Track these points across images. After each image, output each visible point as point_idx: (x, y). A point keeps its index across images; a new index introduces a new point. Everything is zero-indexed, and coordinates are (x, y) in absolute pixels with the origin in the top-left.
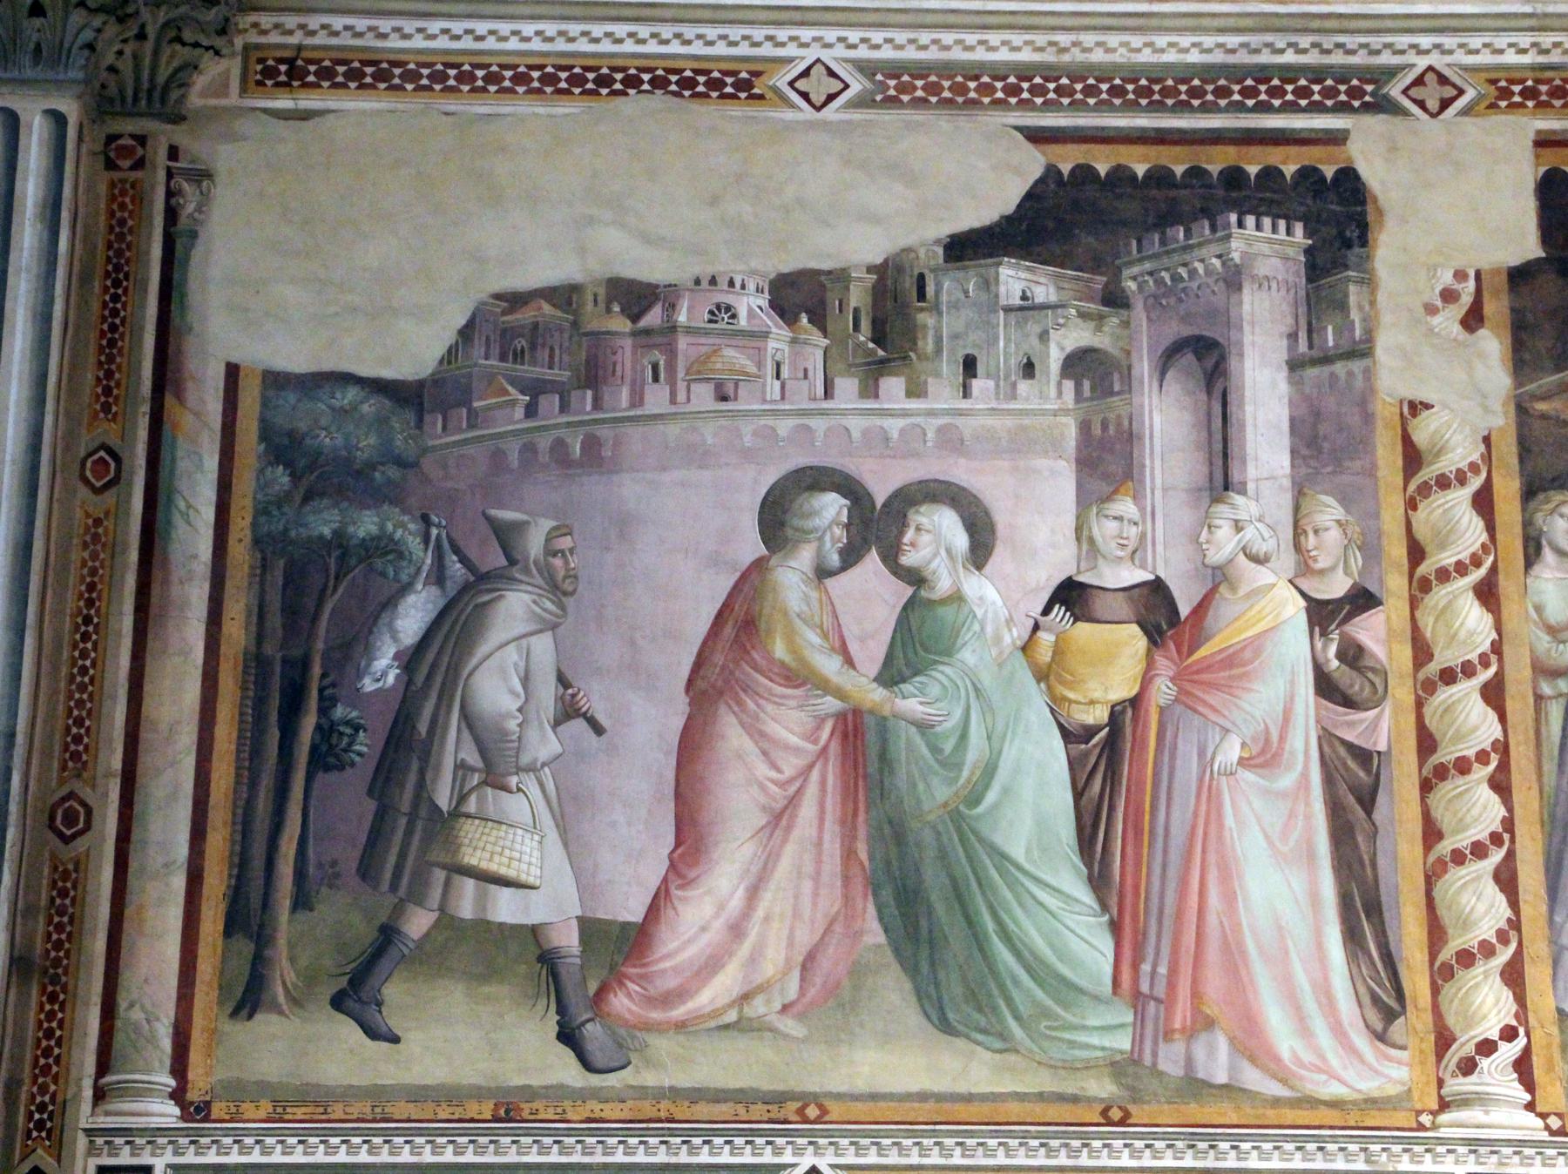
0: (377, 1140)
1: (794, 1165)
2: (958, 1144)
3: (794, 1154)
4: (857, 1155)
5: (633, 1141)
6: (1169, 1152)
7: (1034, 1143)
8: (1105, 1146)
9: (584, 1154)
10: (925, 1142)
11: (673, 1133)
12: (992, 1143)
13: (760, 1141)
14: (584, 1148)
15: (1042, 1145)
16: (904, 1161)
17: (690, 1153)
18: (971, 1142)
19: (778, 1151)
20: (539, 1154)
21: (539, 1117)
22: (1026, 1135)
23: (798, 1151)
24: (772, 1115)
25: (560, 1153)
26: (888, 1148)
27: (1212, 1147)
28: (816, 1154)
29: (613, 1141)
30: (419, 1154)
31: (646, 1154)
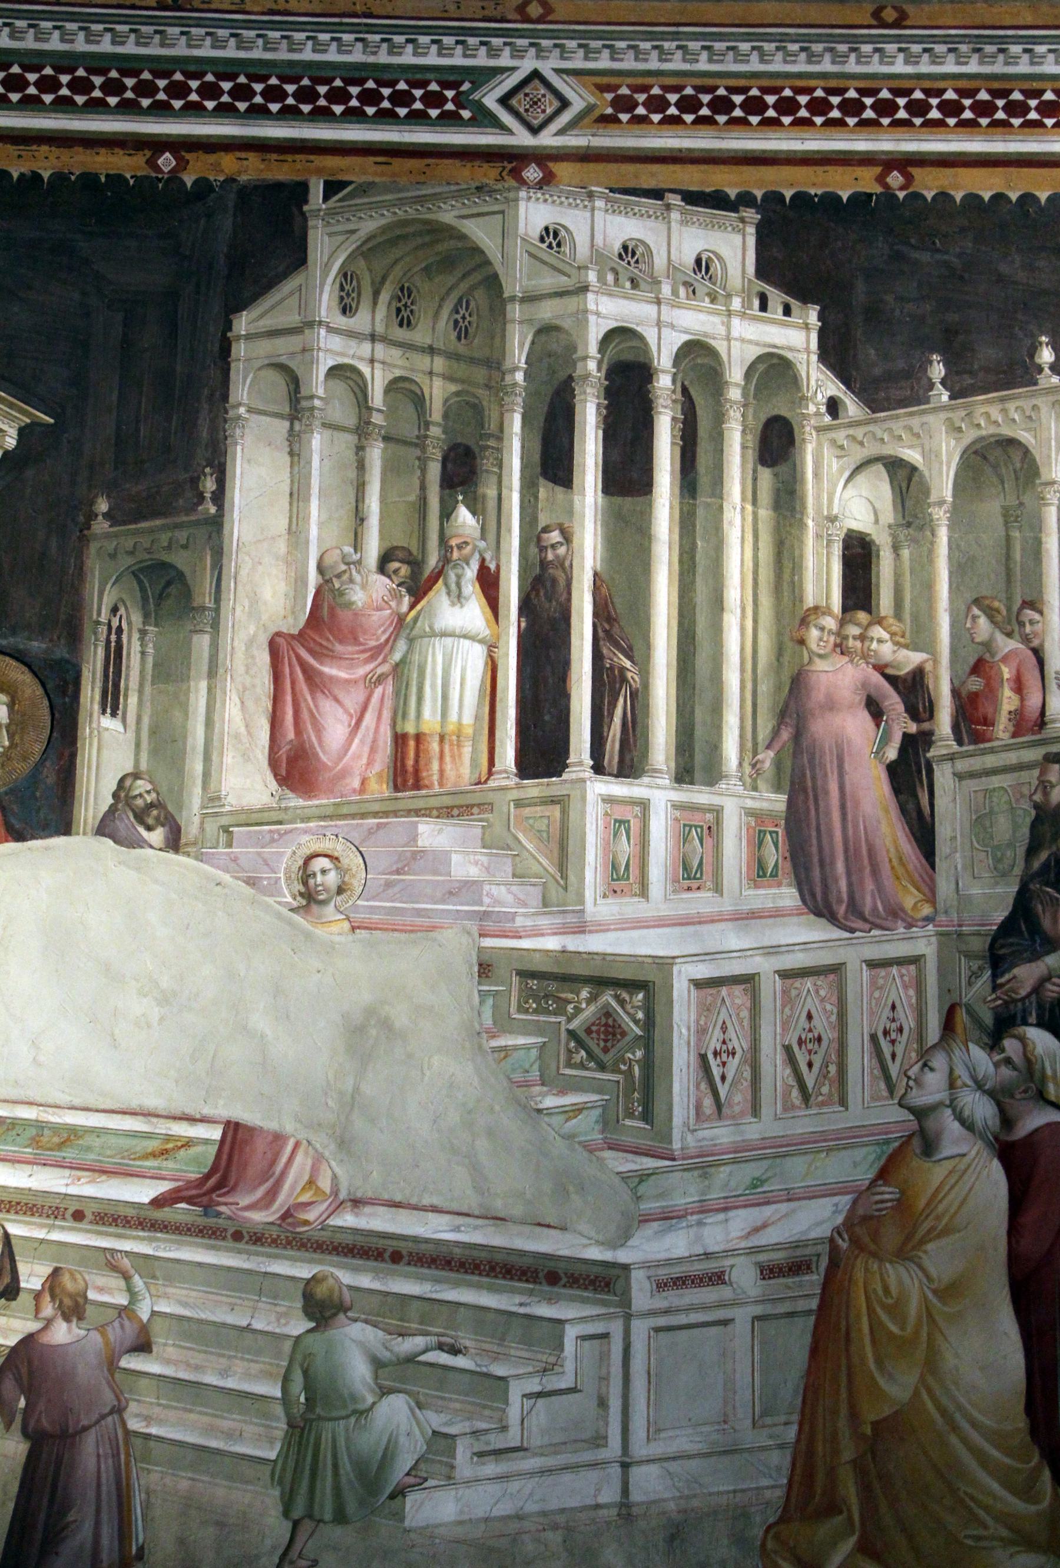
0: (21, 24)
1: (513, 69)
2: (704, 48)
3: (512, 57)
4: (586, 58)
5: (324, 37)
6: (951, 57)
7: (794, 47)
8: (876, 50)
9: (266, 49)
10: (666, 45)
11: (372, 29)
12: (745, 47)
13: (472, 41)
14: (266, 43)
15: (803, 49)
16: (641, 66)
17: (390, 53)
18: (719, 46)
19: (494, 53)
20: (213, 47)
21: (213, 6)
22: (784, 38)
23: (518, 53)
24: (486, 13)
25: (238, 48)
26: (623, 52)
27: (1002, 51)
28: (538, 57)
29: (300, 36)
30: (72, 41)
31: (339, 51)
